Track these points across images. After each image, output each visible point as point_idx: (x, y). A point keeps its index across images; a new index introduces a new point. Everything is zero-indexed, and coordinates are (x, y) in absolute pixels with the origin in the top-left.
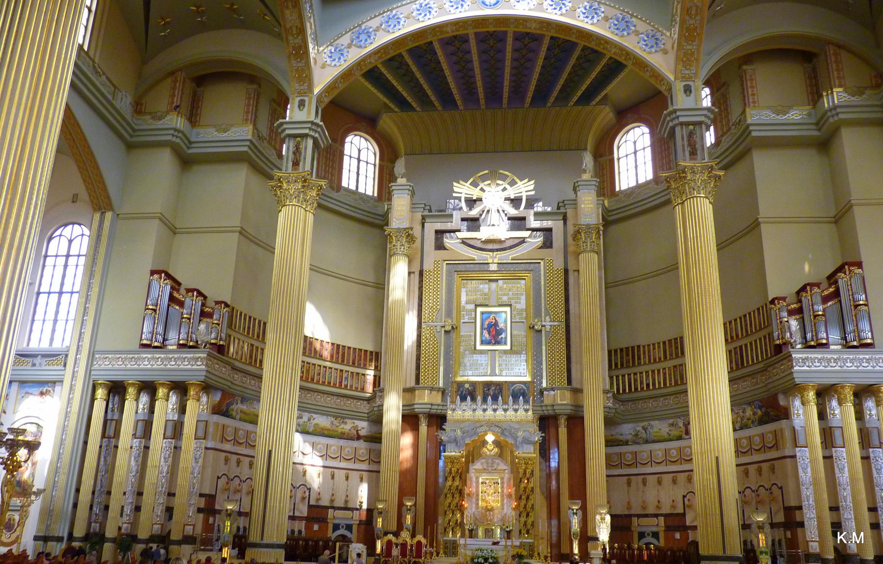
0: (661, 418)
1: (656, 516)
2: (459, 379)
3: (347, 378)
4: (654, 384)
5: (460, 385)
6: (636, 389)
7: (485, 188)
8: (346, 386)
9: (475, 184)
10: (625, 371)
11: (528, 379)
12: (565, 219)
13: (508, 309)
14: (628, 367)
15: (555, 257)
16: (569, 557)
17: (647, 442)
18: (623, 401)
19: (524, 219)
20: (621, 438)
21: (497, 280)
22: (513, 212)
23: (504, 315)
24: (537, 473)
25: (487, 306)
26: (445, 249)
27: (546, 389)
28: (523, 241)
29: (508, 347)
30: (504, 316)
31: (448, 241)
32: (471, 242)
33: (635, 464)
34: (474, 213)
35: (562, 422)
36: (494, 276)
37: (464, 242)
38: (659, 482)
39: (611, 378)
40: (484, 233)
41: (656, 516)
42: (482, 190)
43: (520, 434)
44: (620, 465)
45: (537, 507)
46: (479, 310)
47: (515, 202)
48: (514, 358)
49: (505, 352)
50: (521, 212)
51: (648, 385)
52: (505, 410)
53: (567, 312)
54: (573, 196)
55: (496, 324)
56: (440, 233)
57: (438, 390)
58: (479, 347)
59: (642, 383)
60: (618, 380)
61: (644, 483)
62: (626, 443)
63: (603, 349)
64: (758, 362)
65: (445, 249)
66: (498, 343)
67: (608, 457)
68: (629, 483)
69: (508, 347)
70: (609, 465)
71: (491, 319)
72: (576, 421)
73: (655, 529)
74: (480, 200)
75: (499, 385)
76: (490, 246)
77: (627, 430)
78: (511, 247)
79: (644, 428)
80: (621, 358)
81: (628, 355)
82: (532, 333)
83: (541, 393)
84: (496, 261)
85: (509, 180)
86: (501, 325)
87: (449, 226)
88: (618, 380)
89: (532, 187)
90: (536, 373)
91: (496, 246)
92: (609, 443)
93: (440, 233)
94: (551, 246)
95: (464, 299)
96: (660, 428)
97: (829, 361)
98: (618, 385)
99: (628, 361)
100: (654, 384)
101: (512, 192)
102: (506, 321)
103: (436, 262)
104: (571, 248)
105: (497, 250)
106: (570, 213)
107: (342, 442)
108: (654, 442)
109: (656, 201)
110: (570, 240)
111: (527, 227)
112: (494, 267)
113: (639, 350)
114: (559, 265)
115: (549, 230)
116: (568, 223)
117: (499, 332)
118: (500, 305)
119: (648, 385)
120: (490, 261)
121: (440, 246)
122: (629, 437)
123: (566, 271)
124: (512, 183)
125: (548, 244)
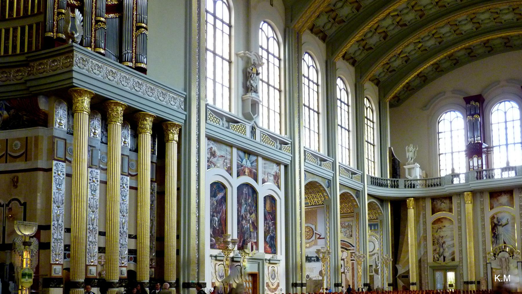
64: (14, 54)
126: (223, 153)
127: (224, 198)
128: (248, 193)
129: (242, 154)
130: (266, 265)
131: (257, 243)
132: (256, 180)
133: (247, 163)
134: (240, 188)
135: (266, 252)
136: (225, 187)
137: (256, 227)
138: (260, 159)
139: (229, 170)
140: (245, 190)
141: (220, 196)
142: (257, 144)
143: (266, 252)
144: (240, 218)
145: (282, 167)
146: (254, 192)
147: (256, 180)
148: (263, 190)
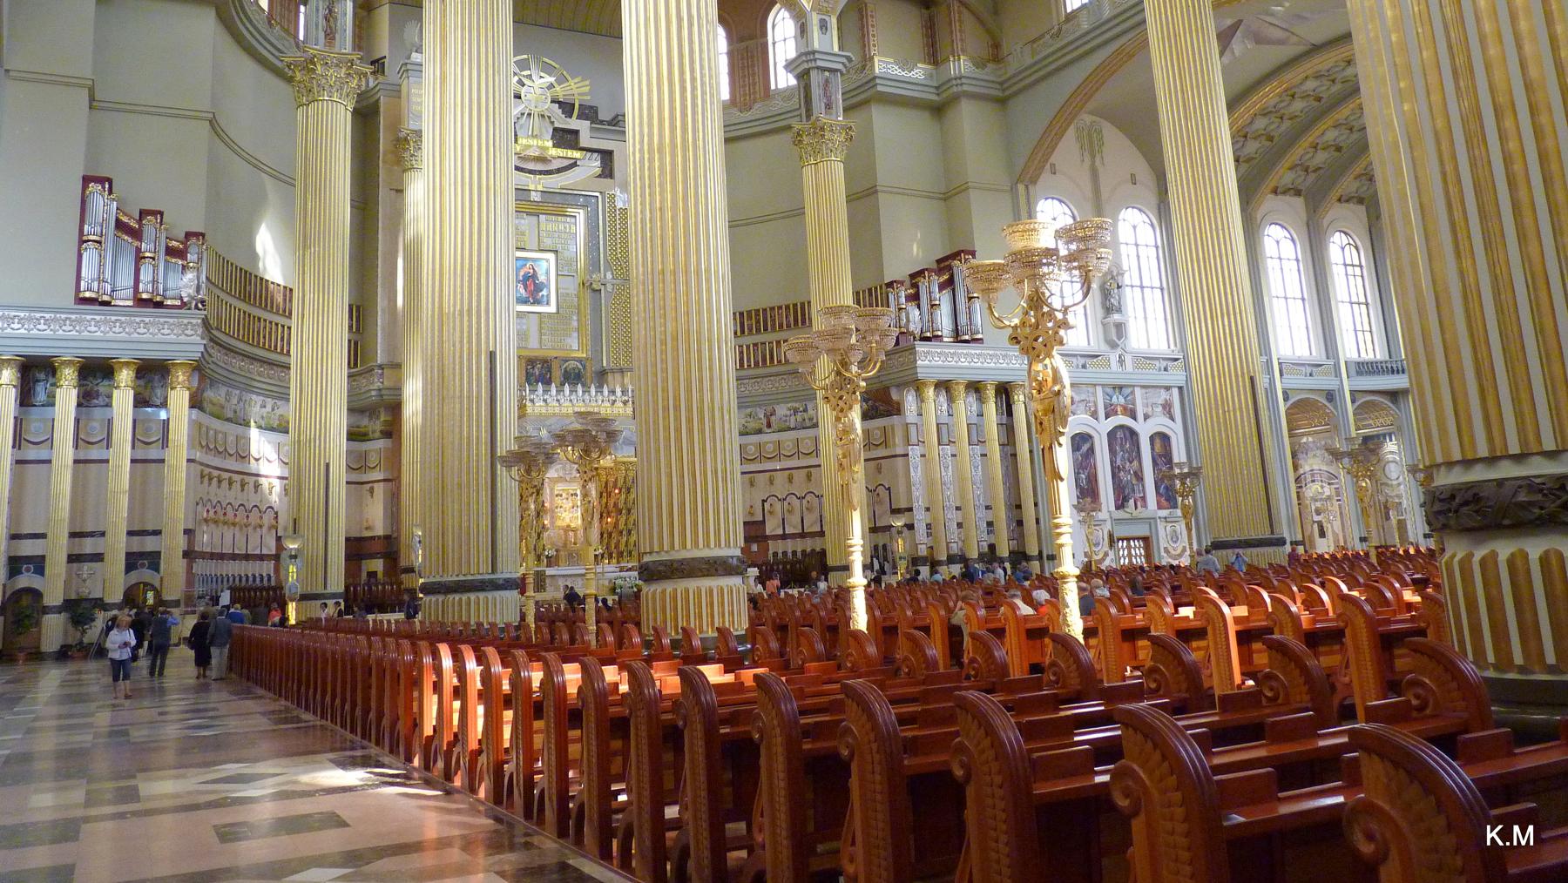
7: (526, 81)
13: (551, 256)
19: (576, 132)
23: (544, 264)
29: (552, 309)
30: (546, 267)
36: (532, 209)
47: (567, 108)
50: (574, 123)
55: (534, 276)
66: (537, 302)
69: (552, 309)
71: (527, 269)
76: (531, 166)
78: (559, 171)
82: (588, 293)
86: (542, 278)
91: (540, 167)
97: (946, 355)
101: (560, 91)
102: (548, 273)
105: (541, 172)
111: (583, 144)
115: (610, 153)
117: (539, 288)
120: (532, 187)
124: (561, 80)
126: (1083, 397)
127: (1092, 450)
128: (1123, 439)
129: (1109, 390)
130: (1161, 526)
131: (1144, 499)
132: (1135, 418)
133: (1118, 399)
134: (1111, 435)
135: (1160, 507)
136: (1090, 437)
137: (1139, 477)
138: (1137, 390)
139: (1094, 415)
140: (1119, 434)
141: (1085, 448)
142: (1128, 372)
143: (1160, 507)
144: (1115, 471)
145: (1175, 392)
146: (1133, 434)
147: (1135, 418)
148: (1145, 430)
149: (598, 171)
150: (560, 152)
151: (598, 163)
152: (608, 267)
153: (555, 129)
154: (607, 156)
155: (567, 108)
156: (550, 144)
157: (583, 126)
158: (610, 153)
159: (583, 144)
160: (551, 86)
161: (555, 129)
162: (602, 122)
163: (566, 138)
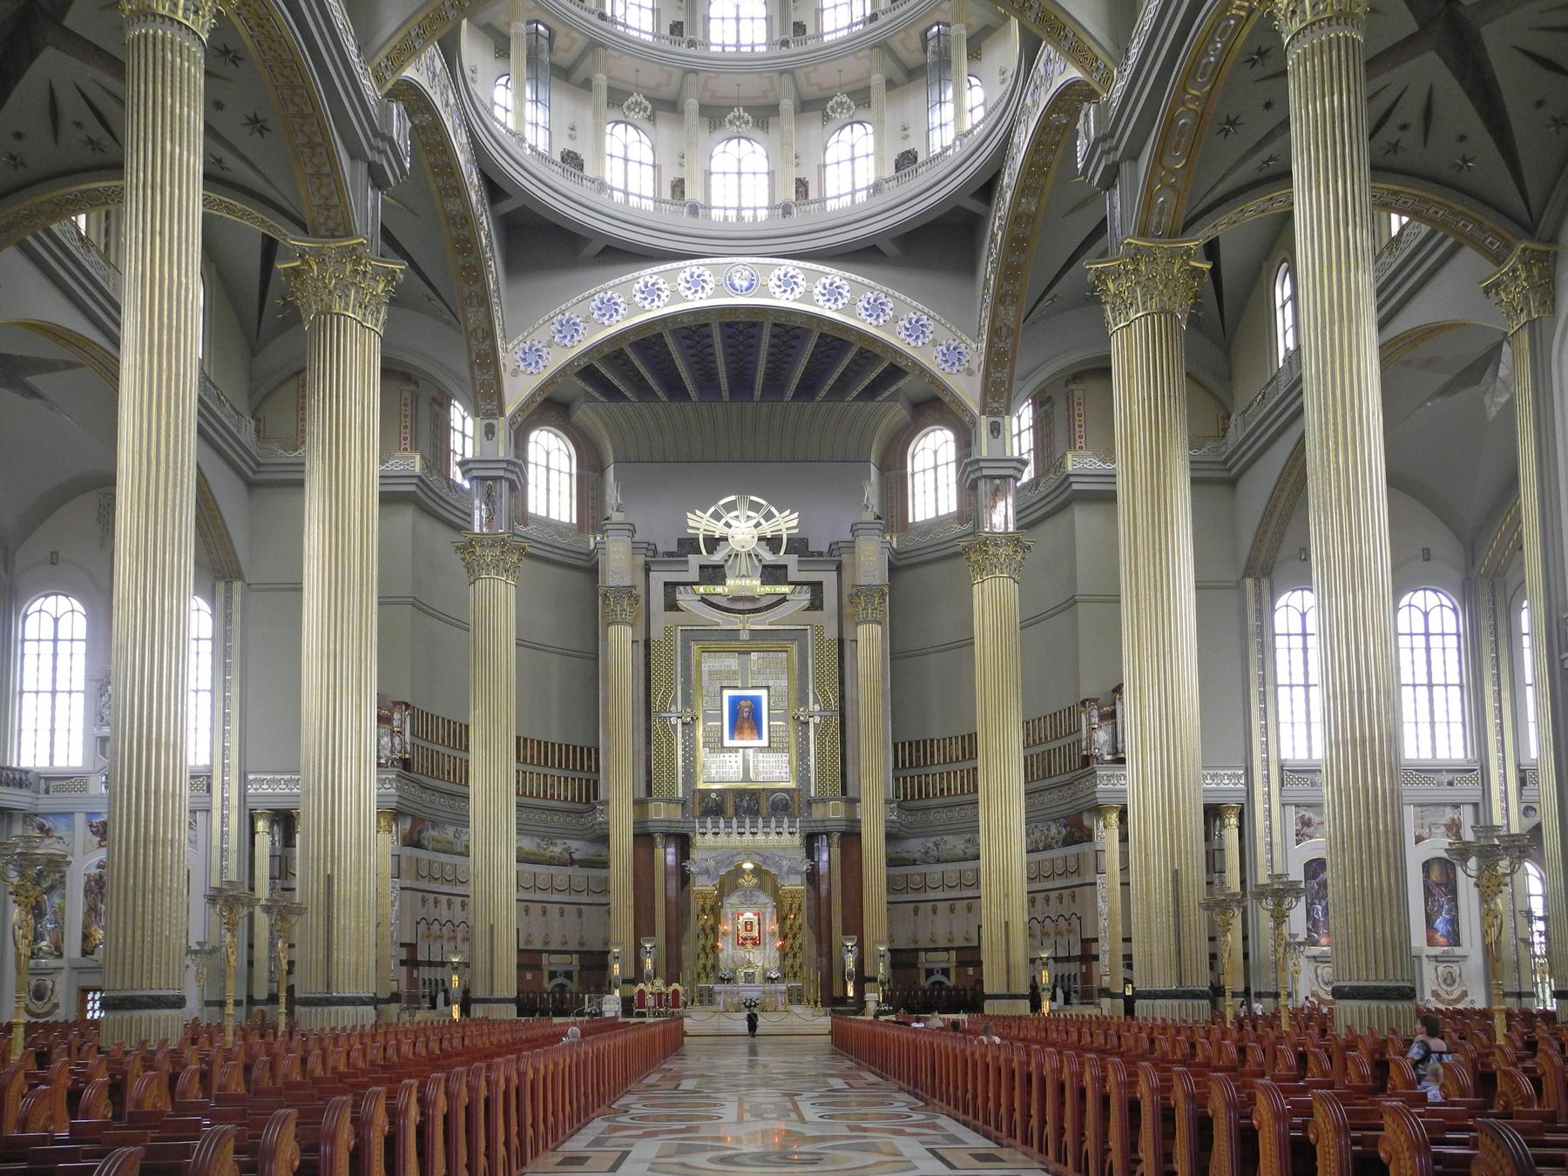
0: (956, 833)
1: (947, 950)
2: (701, 786)
3: (552, 785)
4: (949, 789)
5: (705, 793)
6: (927, 795)
7: (732, 522)
8: (552, 796)
9: (717, 516)
10: (914, 772)
11: (792, 785)
12: (839, 569)
14: (918, 766)
15: (827, 620)
16: (843, 999)
17: (938, 861)
18: (912, 811)
20: (905, 855)
21: (749, 653)
22: (769, 557)
24: (804, 907)
25: (736, 688)
26: (679, 610)
27: (816, 801)
28: (783, 599)
31: (683, 598)
32: (714, 600)
33: (924, 888)
34: (717, 558)
35: (836, 838)
36: (745, 647)
37: (704, 600)
38: (952, 910)
39: (897, 779)
40: (733, 585)
41: (947, 950)
42: (728, 525)
43: (785, 863)
44: (905, 890)
45: (805, 945)
46: (727, 693)
48: (772, 758)
49: (761, 749)
50: (782, 558)
51: (942, 790)
52: (767, 834)
53: (842, 698)
54: (849, 537)
56: (670, 586)
57: (677, 801)
58: (728, 742)
59: (934, 787)
60: (905, 782)
61: (934, 911)
62: (914, 862)
63: (886, 746)
65: (679, 610)
67: (891, 880)
68: (916, 911)
69: (764, 742)
70: (891, 888)
72: (851, 837)
73: (944, 965)
74: (726, 539)
75: (754, 794)
76: (739, 606)
77: (915, 846)
78: (768, 608)
79: (936, 845)
80: (910, 755)
81: (918, 750)
83: (809, 804)
84: (749, 626)
85: (764, 512)
87: (682, 577)
88: (905, 782)
89: (795, 523)
90: (803, 778)
91: (748, 606)
92: (891, 862)
93: (670, 586)
94: (821, 608)
95: (705, 677)
96: (955, 844)
98: (905, 789)
99: (918, 759)
100: (949, 789)
101: (767, 529)
103: (667, 630)
104: (848, 610)
106: (845, 558)
107: (553, 870)
108: (947, 861)
109: (959, 545)
110: (845, 599)
111: (790, 579)
112: (745, 636)
113: (932, 746)
114: (831, 633)
115: (821, 583)
116: (846, 574)
118: (754, 687)
119: (942, 790)
120: (740, 627)
121: (672, 606)
122: (917, 855)
123: (841, 641)
124: (769, 516)
125: (816, 604)
149: (806, 603)
150: (768, 589)
151: (808, 596)
152: (816, 701)
153: (764, 567)
154: (816, 587)
155: (773, 543)
156: (757, 582)
157: (791, 561)
158: (821, 583)
159: (790, 579)
160: (758, 525)
161: (764, 567)
162: (812, 554)
163: (773, 574)
